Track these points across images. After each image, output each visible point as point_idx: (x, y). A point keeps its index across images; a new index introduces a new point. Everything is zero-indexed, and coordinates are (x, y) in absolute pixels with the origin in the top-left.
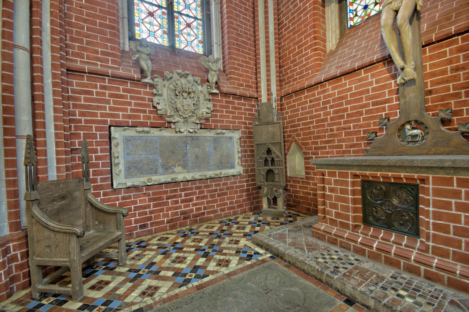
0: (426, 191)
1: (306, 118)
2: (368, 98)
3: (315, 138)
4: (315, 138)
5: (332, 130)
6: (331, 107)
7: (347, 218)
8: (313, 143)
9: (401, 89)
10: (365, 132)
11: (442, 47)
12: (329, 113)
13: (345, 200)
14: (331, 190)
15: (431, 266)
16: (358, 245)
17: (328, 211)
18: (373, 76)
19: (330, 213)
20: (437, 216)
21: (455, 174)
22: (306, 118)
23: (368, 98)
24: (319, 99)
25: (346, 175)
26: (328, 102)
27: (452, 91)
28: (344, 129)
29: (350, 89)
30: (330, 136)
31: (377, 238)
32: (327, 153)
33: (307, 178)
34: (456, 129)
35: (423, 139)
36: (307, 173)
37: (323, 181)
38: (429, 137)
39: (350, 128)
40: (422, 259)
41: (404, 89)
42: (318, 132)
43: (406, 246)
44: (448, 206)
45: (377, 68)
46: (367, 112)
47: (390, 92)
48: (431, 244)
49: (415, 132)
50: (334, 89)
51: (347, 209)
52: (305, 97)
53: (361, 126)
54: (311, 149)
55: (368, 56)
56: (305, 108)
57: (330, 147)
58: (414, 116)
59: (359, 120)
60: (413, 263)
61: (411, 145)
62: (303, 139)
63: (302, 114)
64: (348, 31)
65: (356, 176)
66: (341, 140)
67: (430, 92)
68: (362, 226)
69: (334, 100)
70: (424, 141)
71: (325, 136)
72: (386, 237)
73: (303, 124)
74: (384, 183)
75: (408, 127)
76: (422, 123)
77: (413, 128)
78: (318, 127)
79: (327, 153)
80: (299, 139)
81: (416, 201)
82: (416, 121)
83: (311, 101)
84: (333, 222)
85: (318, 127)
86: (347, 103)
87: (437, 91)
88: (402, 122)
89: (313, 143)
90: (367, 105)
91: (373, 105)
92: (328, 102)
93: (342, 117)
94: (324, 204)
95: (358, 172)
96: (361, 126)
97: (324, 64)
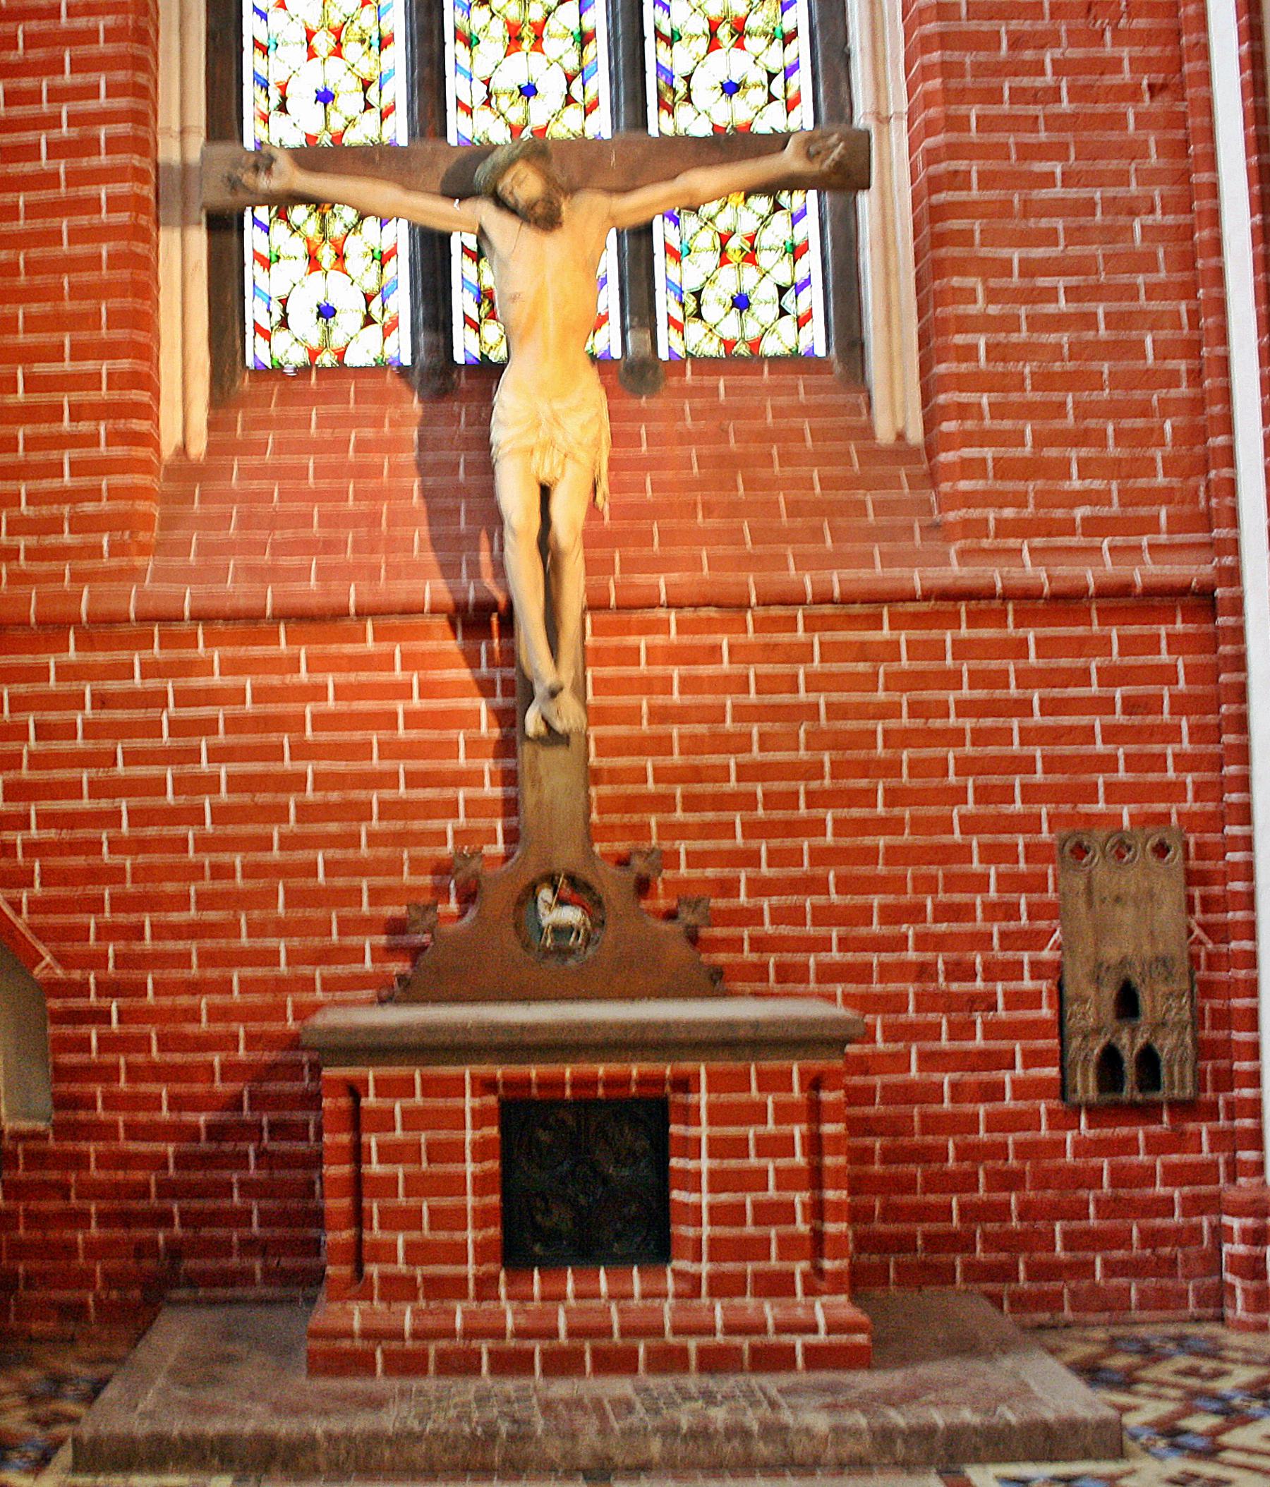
0: (689, 1114)
1: (72, 790)
2: (391, 750)
3: (119, 904)
4: (119, 904)
5: (223, 872)
6: (217, 755)
7: (457, 1253)
8: (106, 932)
9: (526, 751)
10: (377, 896)
11: (626, 629)
12: (211, 783)
13: (454, 1185)
14: (389, 1154)
15: (711, 1331)
16: (511, 1343)
17: (377, 1246)
18: (410, 662)
19: (387, 1252)
20: (720, 1181)
21: (754, 1058)
22: (72, 790)
23: (391, 750)
24: (158, 699)
25: (454, 1087)
26: (208, 727)
27: (651, 786)
28: (281, 870)
29: (318, 693)
30: (205, 902)
31: (562, 1297)
32: (195, 988)
33: (64, 1130)
34: (671, 915)
35: (588, 940)
36: (61, 1102)
37: (356, 1120)
38: (608, 936)
39: (311, 870)
40: (687, 1319)
41: (536, 753)
42: (140, 874)
43: (644, 1296)
44: (737, 1148)
45: (424, 632)
46: (388, 810)
47: (474, 747)
48: (705, 1268)
49: (571, 915)
50: (231, 667)
51: (453, 1219)
52: (65, 672)
53: (361, 868)
54: (98, 961)
55: (395, 572)
56: (68, 731)
57: (208, 959)
58: (567, 857)
59: (352, 840)
60: (670, 1339)
61: (552, 963)
62: (37, 906)
63: (37, 761)
64: (245, 383)
65: (485, 1085)
66: (271, 927)
67: (595, 776)
68: (502, 1275)
69: (235, 724)
70: (590, 951)
71: (181, 902)
72: (584, 1287)
73: (47, 820)
74: (608, 1102)
75: (546, 894)
76: (588, 887)
77: (561, 902)
78: (142, 846)
79: (195, 988)
80: (16, 906)
81: (661, 1147)
82: (572, 879)
83: (101, 701)
84: (397, 1288)
85: (142, 846)
86: (302, 751)
87: (614, 776)
88: (531, 873)
89: (106, 932)
90: (389, 780)
91: (414, 780)
92: (208, 727)
93: (279, 814)
94: (359, 1218)
95: (499, 1072)
96: (361, 868)
97: (169, 523)
